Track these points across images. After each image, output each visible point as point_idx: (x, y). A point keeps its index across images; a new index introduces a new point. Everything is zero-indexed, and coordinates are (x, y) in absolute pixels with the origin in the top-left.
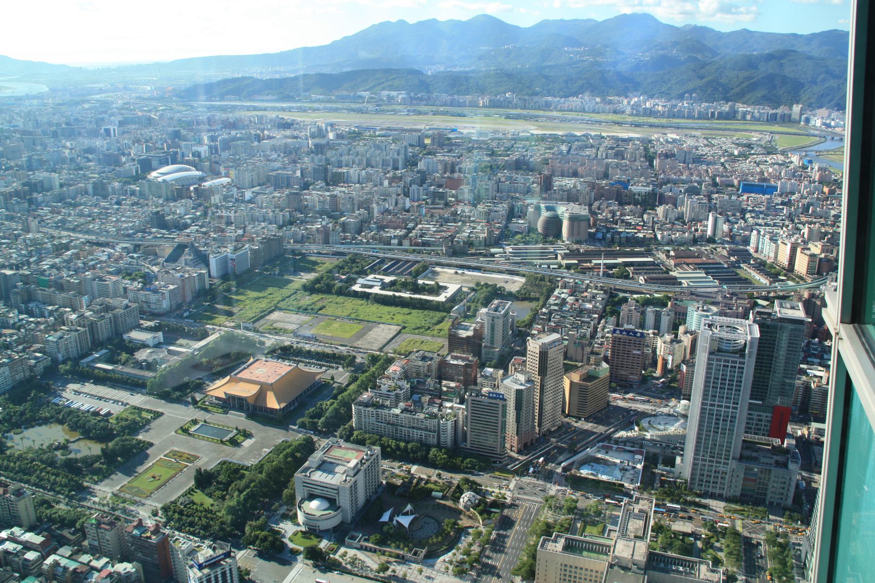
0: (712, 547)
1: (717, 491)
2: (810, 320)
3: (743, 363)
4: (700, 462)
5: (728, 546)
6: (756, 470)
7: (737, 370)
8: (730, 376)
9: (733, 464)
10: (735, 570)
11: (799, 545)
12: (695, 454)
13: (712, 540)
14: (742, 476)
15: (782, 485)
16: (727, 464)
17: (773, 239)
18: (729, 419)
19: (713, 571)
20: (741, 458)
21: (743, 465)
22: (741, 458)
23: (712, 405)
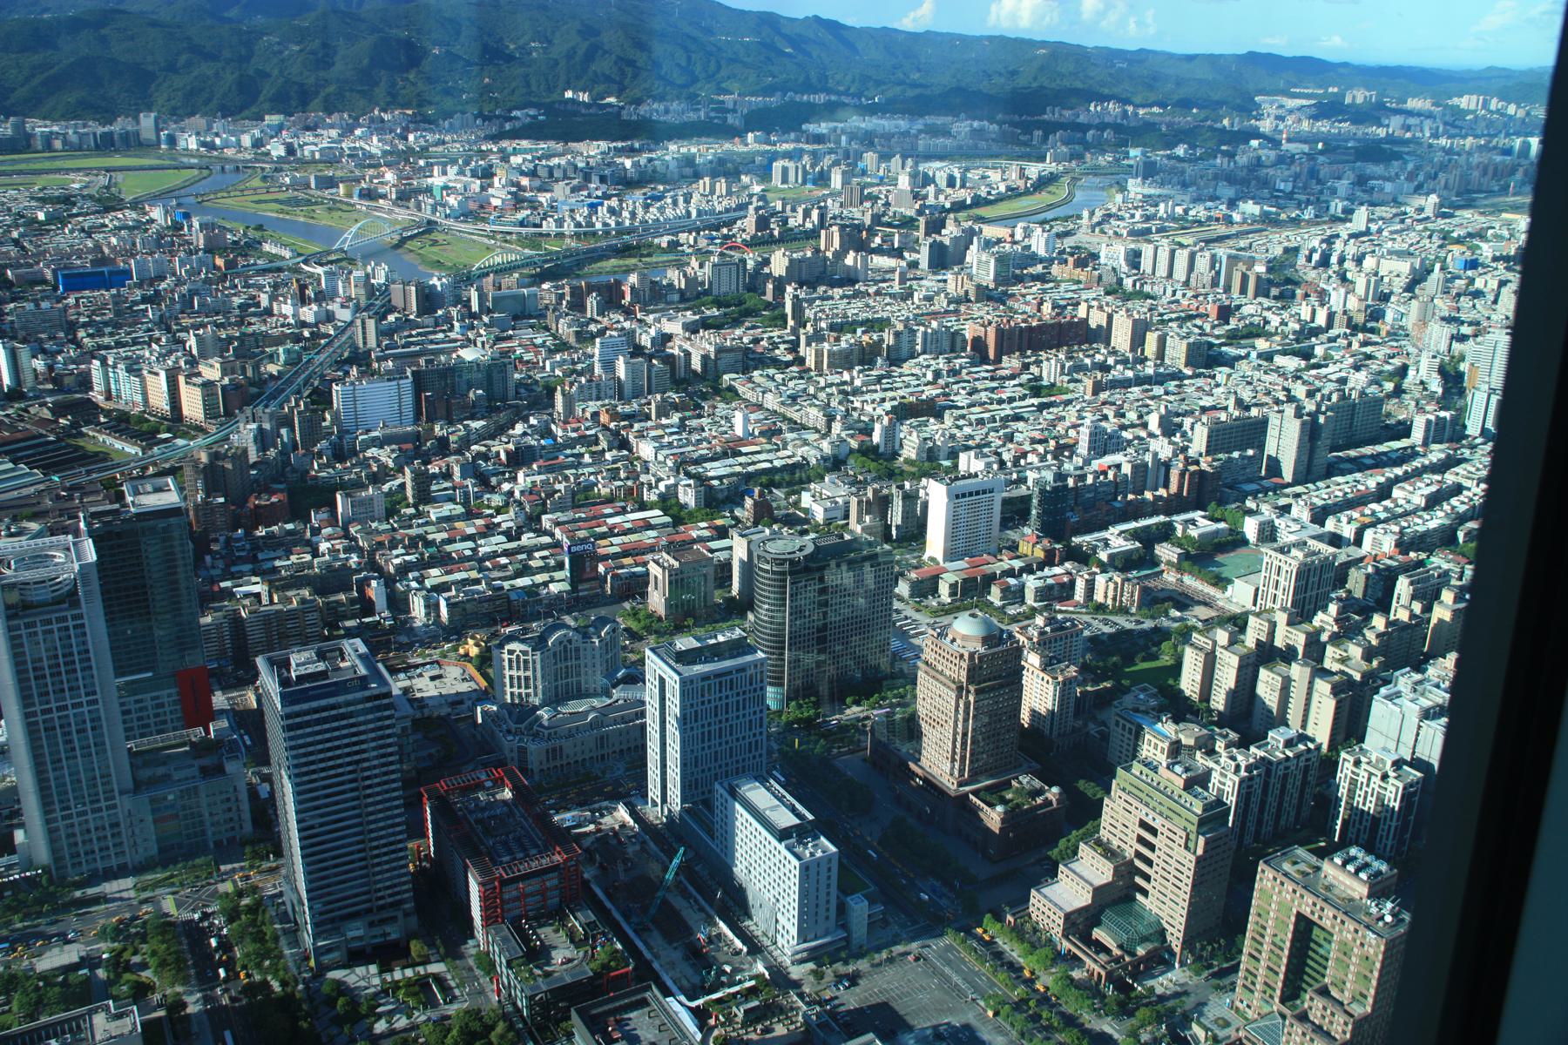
0: (128, 968)
1: (114, 862)
2: (221, 500)
3: (81, 616)
4: (61, 824)
5: (154, 953)
6: (171, 797)
7: (72, 632)
8: (63, 647)
9: (124, 804)
10: (179, 989)
11: (281, 894)
12: (46, 813)
13: (126, 956)
14: (150, 818)
15: (226, 806)
16: (114, 807)
17: (134, 369)
18: (89, 725)
19: (119, 1016)
20: (138, 786)
21: (144, 798)
22: (138, 786)
23: (44, 712)
